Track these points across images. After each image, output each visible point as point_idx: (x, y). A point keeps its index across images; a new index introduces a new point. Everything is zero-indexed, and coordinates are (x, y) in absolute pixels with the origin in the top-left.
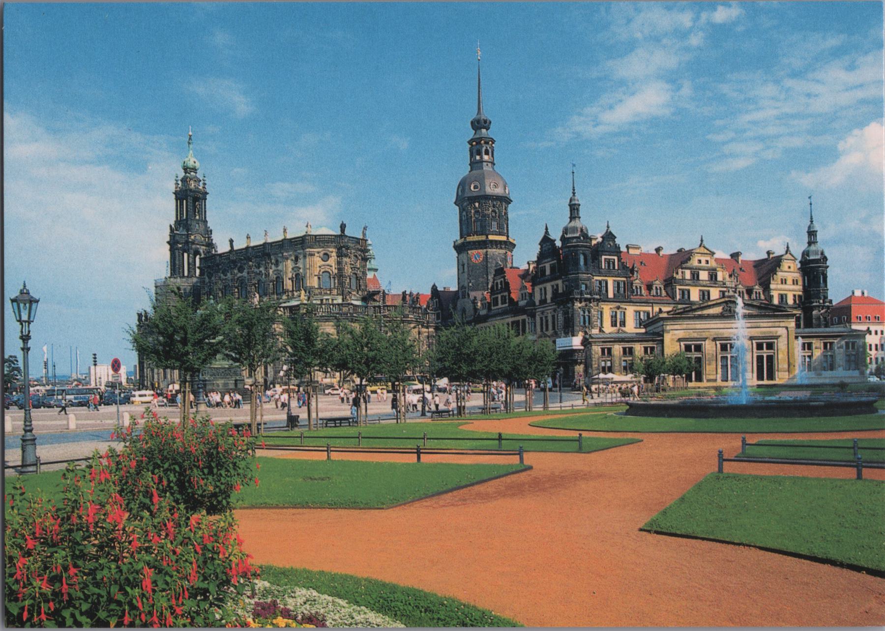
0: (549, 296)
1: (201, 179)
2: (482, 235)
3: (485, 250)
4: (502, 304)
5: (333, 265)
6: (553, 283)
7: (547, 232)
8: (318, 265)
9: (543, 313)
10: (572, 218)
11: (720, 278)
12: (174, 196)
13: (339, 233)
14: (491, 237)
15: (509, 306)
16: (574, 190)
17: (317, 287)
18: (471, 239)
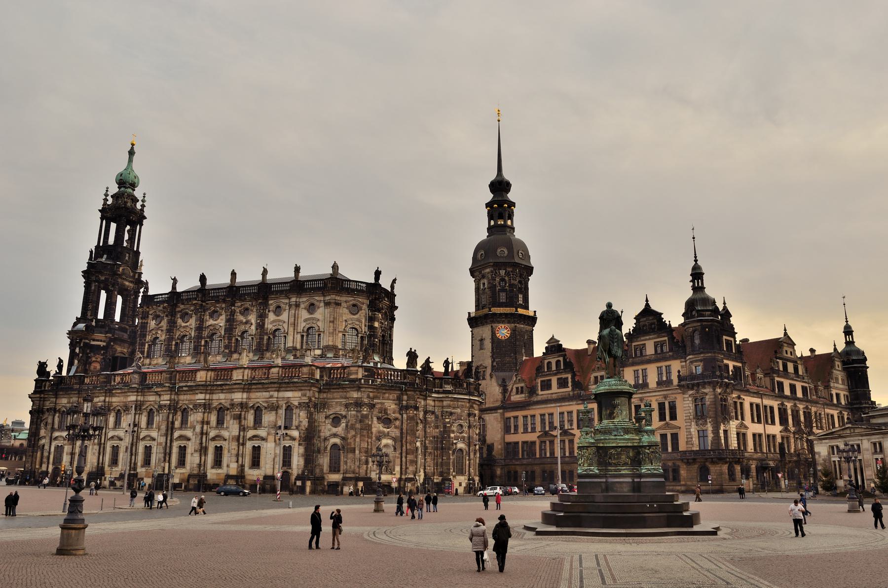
0: (652, 380)
1: (140, 198)
2: (506, 306)
3: (513, 325)
4: (558, 388)
5: (363, 321)
6: (663, 364)
7: (647, 305)
8: (346, 319)
9: (641, 400)
10: (694, 289)
11: (800, 373)
12: (99, 214)
13: (373, 281)
14: (521, 311)
15: (573, 390)
16: (696, 257)
17: (340, 347)
18: (496, 310)
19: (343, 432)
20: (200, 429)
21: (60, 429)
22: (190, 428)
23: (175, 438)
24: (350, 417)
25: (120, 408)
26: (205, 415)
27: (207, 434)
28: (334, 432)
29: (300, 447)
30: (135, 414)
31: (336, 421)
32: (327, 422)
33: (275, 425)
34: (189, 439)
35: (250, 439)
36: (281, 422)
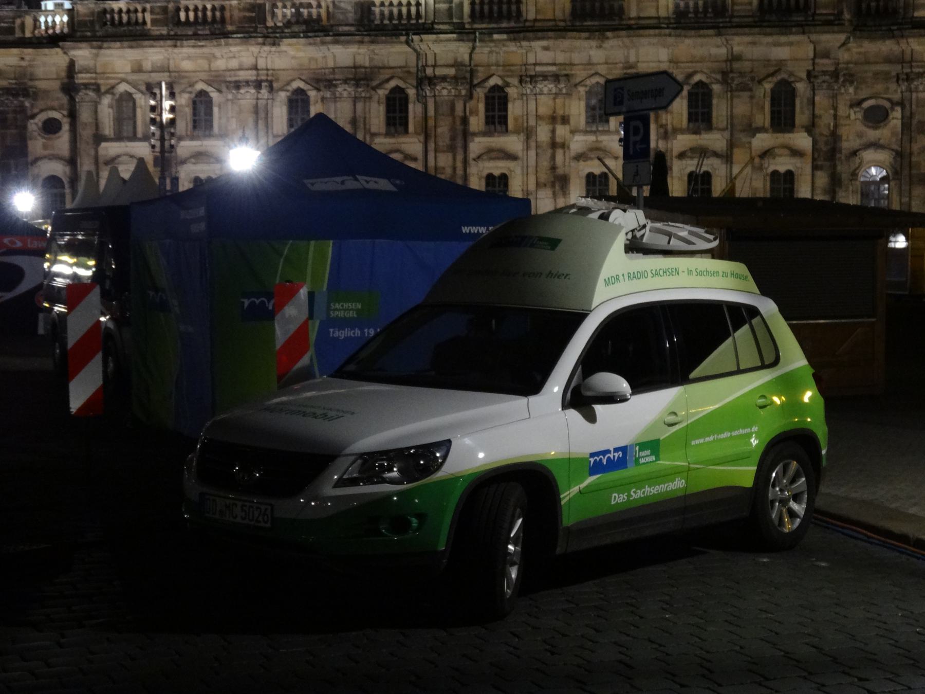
19: (894, 140)
20: (549, 135)
21: (119, 138)
22: (517, 132)
23: (472, 155)
24: (917, 106)
25: (302, 85)
26: (557, 100)
27: (564, 146)
28: (872, 140)
29: (819, 173)
30: (355, 100)
31: (876, 117)
32: (853, 117)
33: (750, 125)
34: (512, 157)
35: (682, 156)
36: (763, 118)
